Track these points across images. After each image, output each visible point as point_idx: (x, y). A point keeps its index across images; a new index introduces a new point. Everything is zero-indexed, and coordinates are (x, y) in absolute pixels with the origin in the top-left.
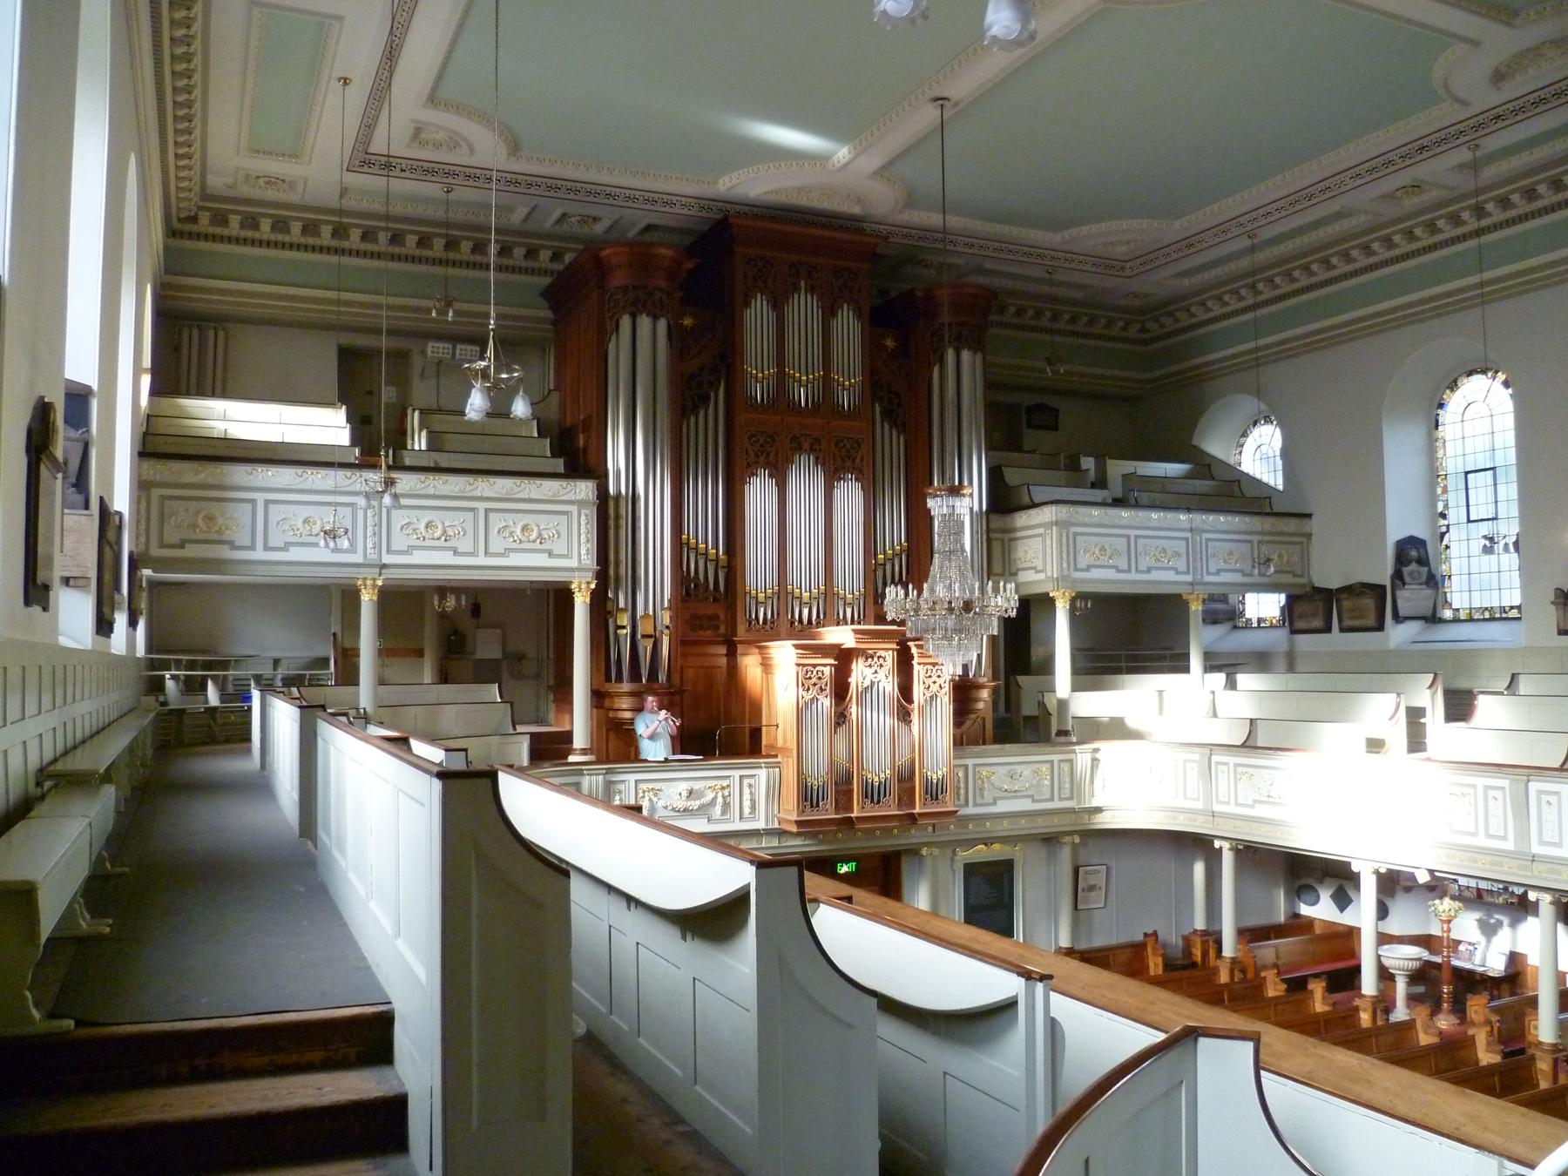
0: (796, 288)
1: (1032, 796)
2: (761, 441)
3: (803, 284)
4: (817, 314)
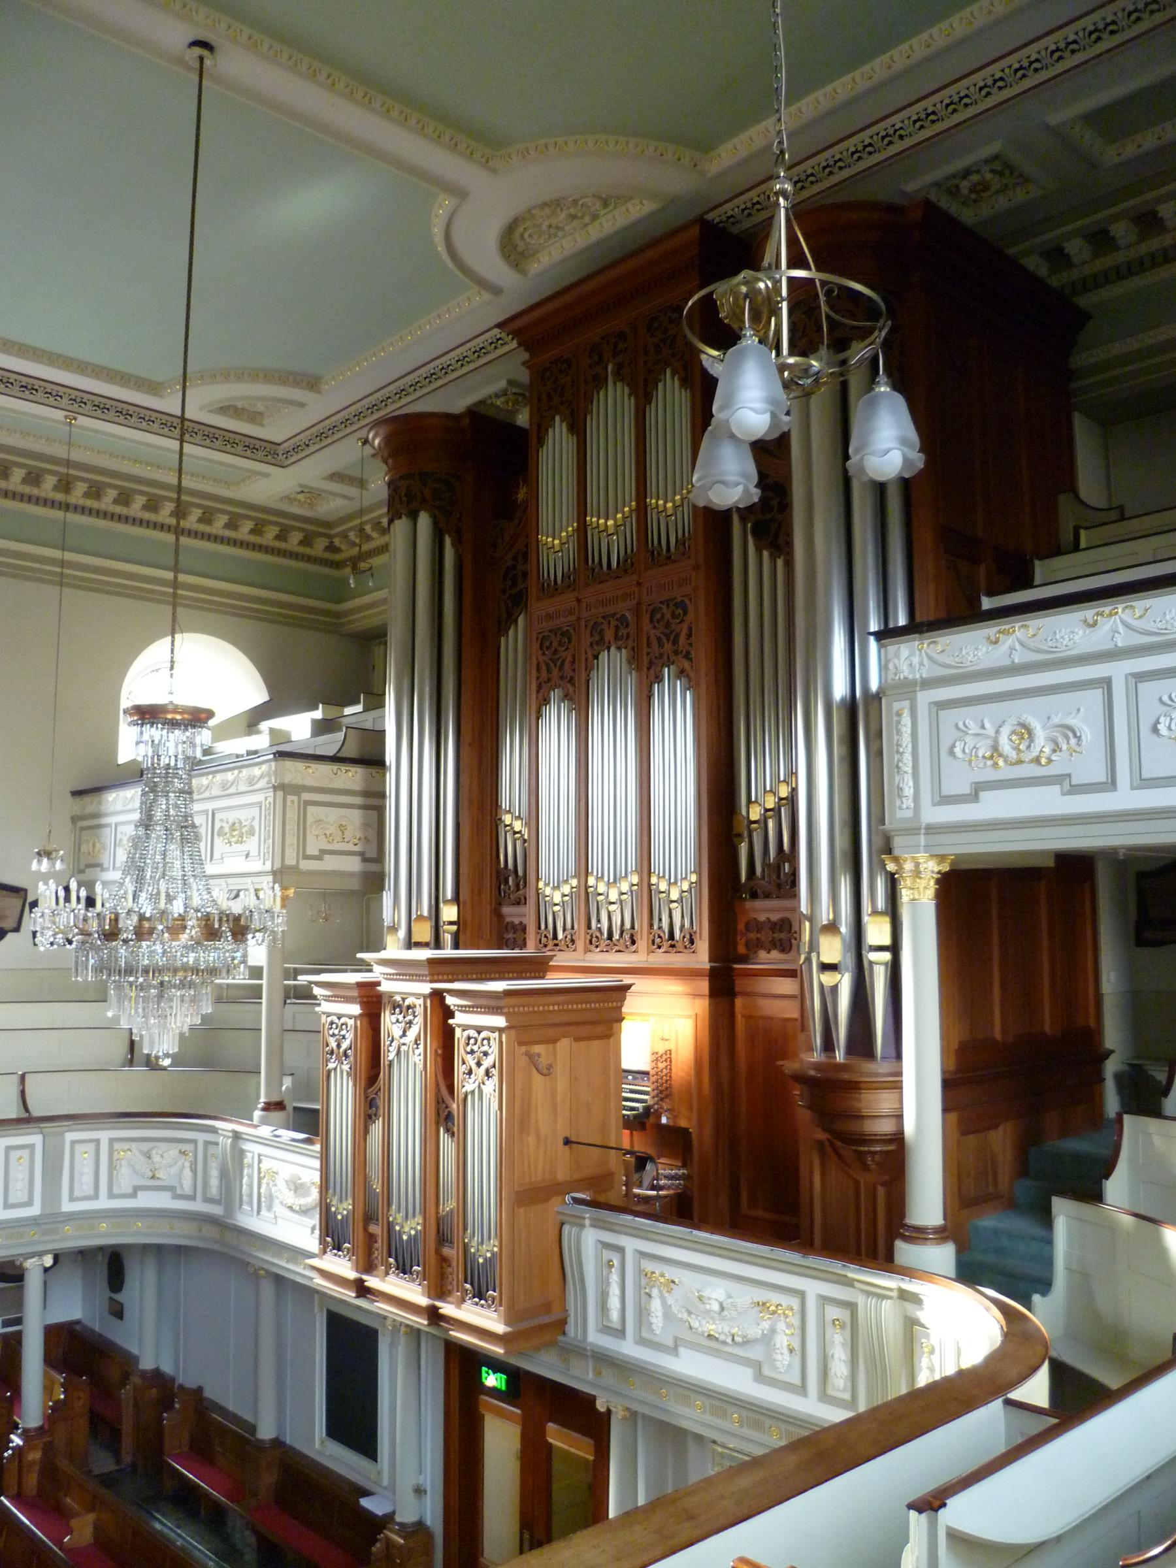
0: (599, 382)
1: (757, 1366)
2: (555, 644)
4: (628, 405)
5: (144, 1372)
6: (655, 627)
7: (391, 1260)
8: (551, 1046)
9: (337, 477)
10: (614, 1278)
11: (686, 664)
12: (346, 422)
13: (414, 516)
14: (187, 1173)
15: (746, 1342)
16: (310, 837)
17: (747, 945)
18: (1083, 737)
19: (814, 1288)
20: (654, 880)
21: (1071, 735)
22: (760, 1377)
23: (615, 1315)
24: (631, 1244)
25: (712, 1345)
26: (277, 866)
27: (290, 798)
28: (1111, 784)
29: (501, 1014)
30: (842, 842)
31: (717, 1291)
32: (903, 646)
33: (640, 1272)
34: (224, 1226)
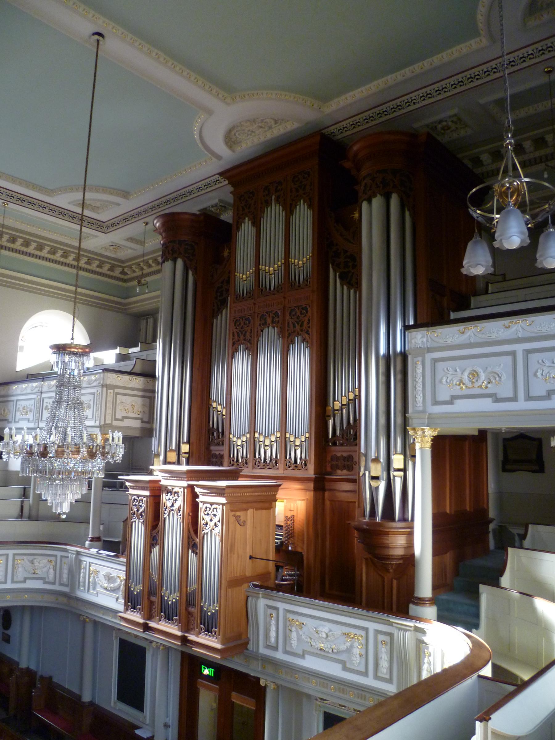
0: (268, 203)
2: (242, 324)
3: (273, 197)
5: (22, 669)
6: (292, 318)
7: (162, 614)
8: (245, 512)
9: (131, 239)
10: (273, 622)
11: (307, 336)
12: (138, 214)
13: (175, 261)
14: (51, 571)
15: (339, 652)
16: (118, 410)
17: (332, 468)
18: (502, 377)
19: (372, 626)
20: (288, 436)
21: (497, 376)
22: (345, 668)
23: (273, 640)
24: (282, 606)
25: (322, 654)
26: (102, 423)
27: (109, 391)
28: (514, 399)
29: (224, 497)
30: (382, 421)
31: (325, 628)
32: (419, 333)
33: (286, 619)
34: (70, 597)
